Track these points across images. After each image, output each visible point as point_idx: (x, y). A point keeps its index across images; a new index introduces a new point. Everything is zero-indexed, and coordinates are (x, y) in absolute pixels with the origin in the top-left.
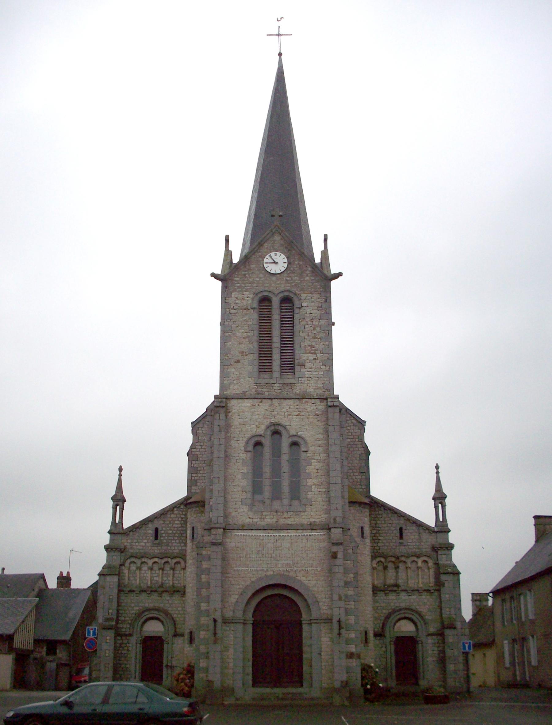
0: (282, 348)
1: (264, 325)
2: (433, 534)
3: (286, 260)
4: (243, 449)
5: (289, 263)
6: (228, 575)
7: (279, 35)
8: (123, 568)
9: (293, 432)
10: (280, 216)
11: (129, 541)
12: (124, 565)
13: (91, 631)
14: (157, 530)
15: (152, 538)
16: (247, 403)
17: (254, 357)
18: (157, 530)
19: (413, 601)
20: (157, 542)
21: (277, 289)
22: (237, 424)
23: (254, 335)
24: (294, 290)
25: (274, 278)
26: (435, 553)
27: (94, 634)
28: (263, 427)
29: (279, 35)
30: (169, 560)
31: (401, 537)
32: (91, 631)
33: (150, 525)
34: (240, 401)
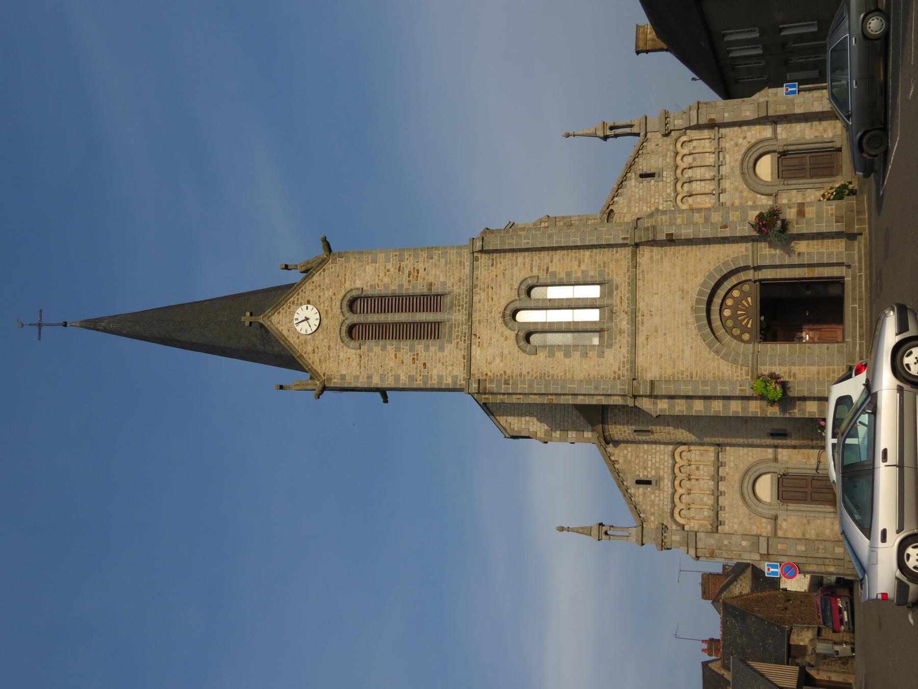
0: (411, 310)
1: (382, 332)
2: (649, 135)
3: (304, 307)
4: (533, 357)
5: (309, 302)
6: (694, 373)
7: (40, 326)
8: (686, 528)
9: (514, 295)
10: (251, 315)
11: (652, 518)
12: (683, 526)
13: (772, 570)
14: (639, 482)
15: (649, 488)
16: (476, 352)
17: (420, 346)
18: (639, 482)
19: (732, 160)
20: (653, 483)
21: (338, 317)
22: (502, 364)
23: (391, 346)
24: (340, 297)
25: (325, 322)
26: (673, 133)
27: (776, 567)
28: (507, 332)
29: (40, 326)
30: (677, 466)
31: (652, 175)
32: (772, 570)
33: (632, 491)
34: (473, 361)
